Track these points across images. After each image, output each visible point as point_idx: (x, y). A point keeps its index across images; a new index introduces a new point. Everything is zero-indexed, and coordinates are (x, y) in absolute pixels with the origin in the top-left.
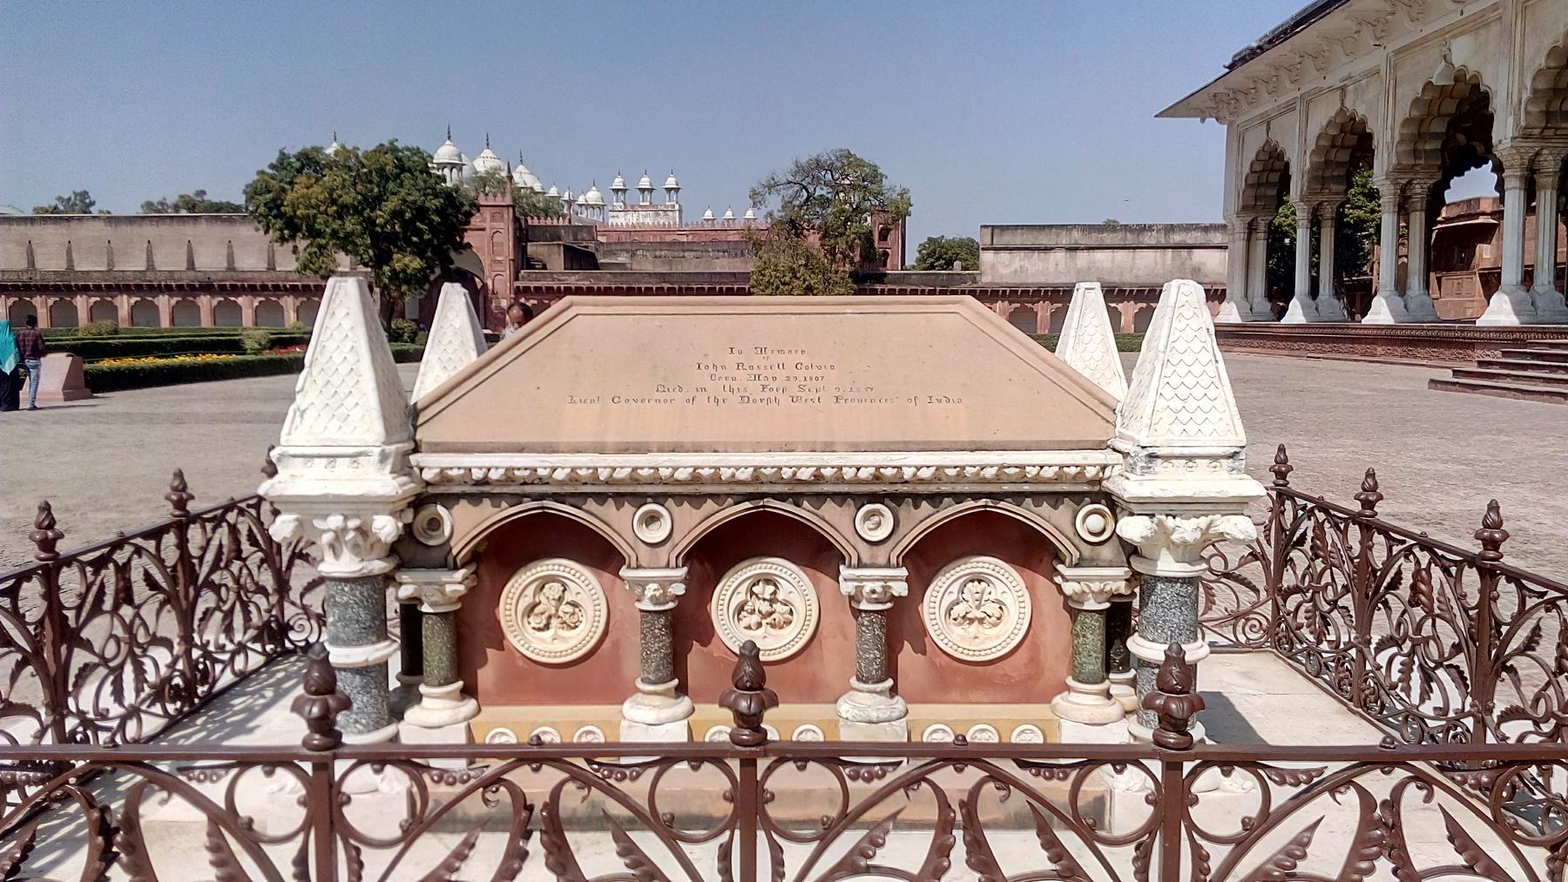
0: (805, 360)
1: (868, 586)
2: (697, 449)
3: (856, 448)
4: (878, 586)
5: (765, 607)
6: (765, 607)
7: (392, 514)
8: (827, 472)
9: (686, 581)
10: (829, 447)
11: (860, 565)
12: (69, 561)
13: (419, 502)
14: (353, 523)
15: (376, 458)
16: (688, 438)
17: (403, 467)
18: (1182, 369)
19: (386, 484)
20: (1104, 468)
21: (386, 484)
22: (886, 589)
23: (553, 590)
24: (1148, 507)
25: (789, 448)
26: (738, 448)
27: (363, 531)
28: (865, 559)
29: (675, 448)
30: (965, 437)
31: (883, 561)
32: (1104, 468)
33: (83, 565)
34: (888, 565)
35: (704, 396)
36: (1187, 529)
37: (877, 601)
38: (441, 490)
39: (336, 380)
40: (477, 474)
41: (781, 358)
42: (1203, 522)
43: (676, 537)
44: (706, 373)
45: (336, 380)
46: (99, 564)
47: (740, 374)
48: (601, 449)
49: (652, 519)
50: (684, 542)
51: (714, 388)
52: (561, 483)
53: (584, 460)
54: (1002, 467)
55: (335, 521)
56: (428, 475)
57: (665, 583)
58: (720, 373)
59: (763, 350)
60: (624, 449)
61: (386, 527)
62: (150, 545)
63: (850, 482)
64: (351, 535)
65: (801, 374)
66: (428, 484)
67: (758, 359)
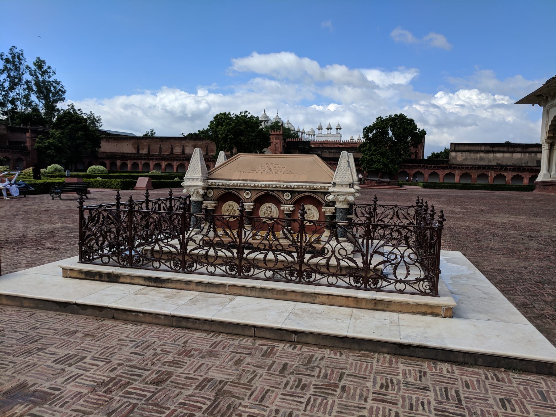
0: (280, 166)
1: (286, 208)
2: (256, 181)
3: (284, 182)
4: (287, 208)
5: (269, 213)
6: (269, 213)
7: (202, 189)
8: (278, 186)
9: (253, 205)
10: (279, 181)
11: (285, 204)
12: (150, 201)
13: (208, 188)
14: (196, 191)
15: (200, 179)
16: (254, 179)
17: (204, 181)
18: (342, 168)
19: (201, 184)
20: (329, 187)
21: (201, 184)
22: (289, 208)
23: (231, 207)
24: (334, 193)
25: (272, 181)
26: (263, 181)
27: (197, 192)
28: (286, 203)
29: (252, 181)
30: (305, 180)
31: (289, 203)
32: (329, 187)
33: (153, 203)
34: (290, 204)
35: (259, 172)
36: (341, 198)
37: (288, 211)
38: (212, 186)
39: (195, 166)
40: (217, 184)
41: (275, 166)
42: (344, 197)
43: (252, 197)
44: (261, 168)
45: (195, 166)
46: (156, 203)
47: (268, 168)
48: (239, 180)
49: (248, 194)
50: (253, 199)
51: (261, 170)
52: (232, 186)
53: (235, 182)
54: (310, 186)
55: (193, 190)
56: (209, 184)
57: (249, 206)
58: (264, 168)
59: (273, 164)
60: (243, 180)
61: (201, 192)
62: (165, 202)
63: (282, 188)
64: (195, 193)
65: (278, 169)
66: (209, 185)
67: (272, 166)
